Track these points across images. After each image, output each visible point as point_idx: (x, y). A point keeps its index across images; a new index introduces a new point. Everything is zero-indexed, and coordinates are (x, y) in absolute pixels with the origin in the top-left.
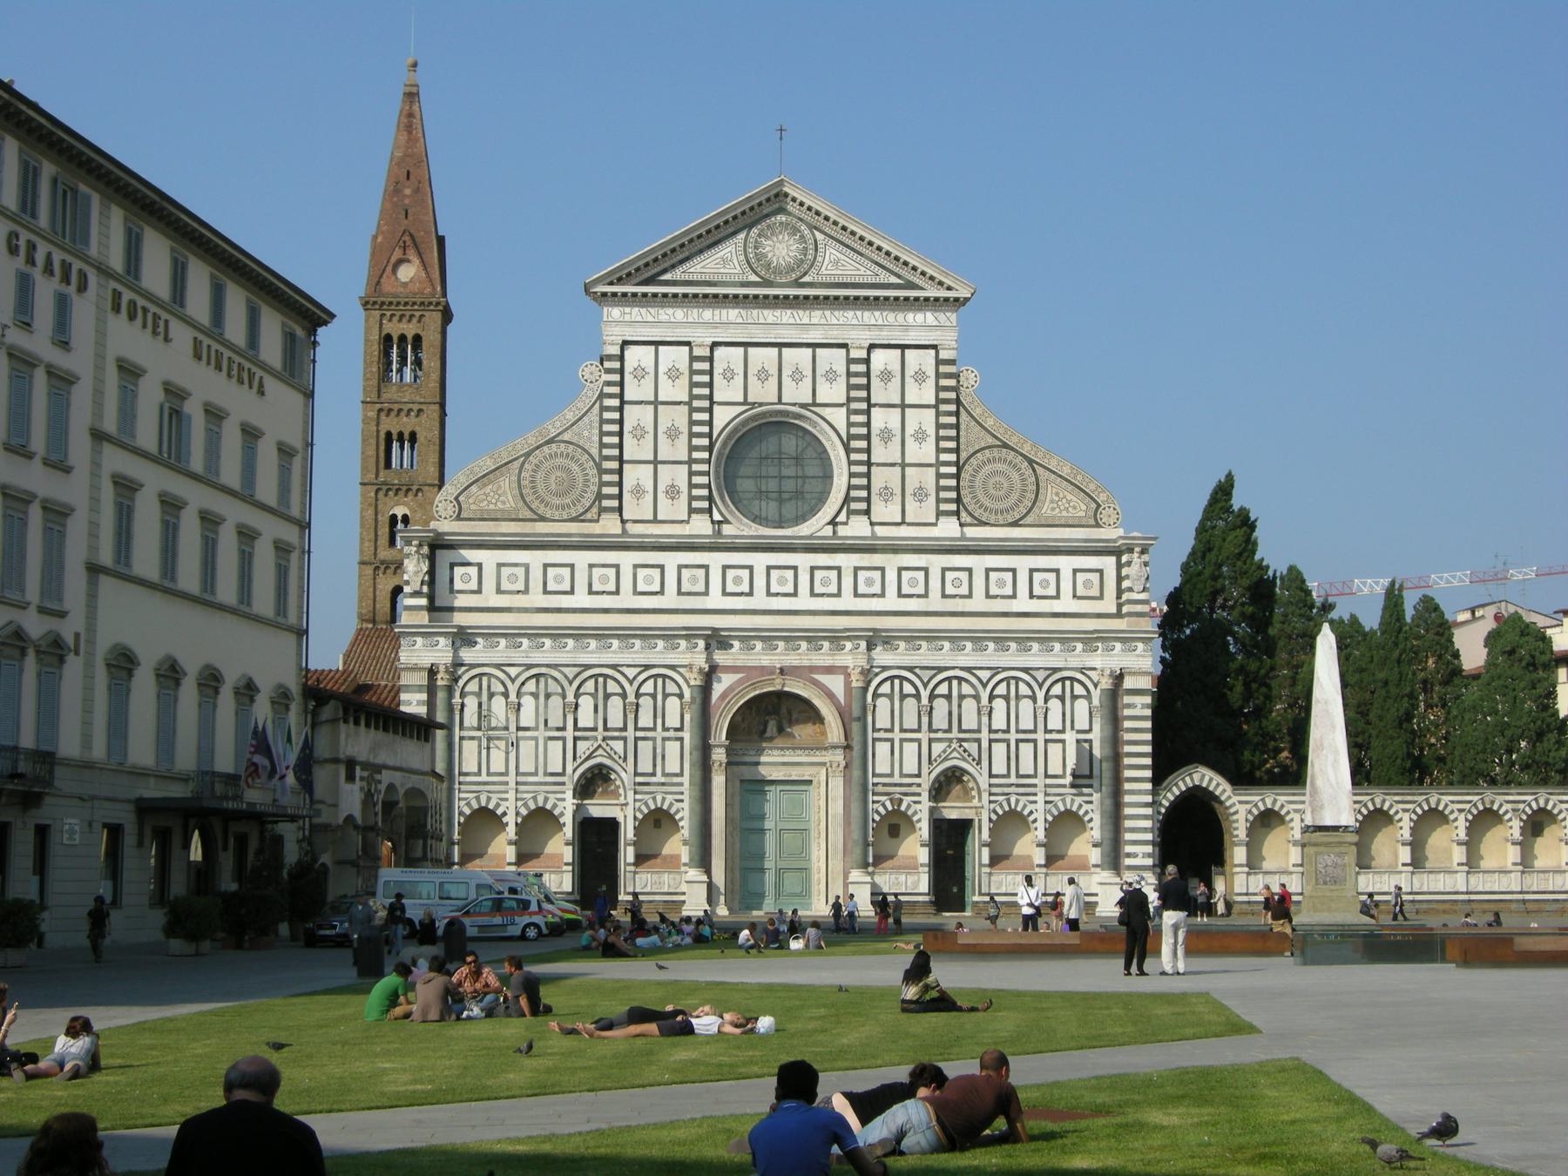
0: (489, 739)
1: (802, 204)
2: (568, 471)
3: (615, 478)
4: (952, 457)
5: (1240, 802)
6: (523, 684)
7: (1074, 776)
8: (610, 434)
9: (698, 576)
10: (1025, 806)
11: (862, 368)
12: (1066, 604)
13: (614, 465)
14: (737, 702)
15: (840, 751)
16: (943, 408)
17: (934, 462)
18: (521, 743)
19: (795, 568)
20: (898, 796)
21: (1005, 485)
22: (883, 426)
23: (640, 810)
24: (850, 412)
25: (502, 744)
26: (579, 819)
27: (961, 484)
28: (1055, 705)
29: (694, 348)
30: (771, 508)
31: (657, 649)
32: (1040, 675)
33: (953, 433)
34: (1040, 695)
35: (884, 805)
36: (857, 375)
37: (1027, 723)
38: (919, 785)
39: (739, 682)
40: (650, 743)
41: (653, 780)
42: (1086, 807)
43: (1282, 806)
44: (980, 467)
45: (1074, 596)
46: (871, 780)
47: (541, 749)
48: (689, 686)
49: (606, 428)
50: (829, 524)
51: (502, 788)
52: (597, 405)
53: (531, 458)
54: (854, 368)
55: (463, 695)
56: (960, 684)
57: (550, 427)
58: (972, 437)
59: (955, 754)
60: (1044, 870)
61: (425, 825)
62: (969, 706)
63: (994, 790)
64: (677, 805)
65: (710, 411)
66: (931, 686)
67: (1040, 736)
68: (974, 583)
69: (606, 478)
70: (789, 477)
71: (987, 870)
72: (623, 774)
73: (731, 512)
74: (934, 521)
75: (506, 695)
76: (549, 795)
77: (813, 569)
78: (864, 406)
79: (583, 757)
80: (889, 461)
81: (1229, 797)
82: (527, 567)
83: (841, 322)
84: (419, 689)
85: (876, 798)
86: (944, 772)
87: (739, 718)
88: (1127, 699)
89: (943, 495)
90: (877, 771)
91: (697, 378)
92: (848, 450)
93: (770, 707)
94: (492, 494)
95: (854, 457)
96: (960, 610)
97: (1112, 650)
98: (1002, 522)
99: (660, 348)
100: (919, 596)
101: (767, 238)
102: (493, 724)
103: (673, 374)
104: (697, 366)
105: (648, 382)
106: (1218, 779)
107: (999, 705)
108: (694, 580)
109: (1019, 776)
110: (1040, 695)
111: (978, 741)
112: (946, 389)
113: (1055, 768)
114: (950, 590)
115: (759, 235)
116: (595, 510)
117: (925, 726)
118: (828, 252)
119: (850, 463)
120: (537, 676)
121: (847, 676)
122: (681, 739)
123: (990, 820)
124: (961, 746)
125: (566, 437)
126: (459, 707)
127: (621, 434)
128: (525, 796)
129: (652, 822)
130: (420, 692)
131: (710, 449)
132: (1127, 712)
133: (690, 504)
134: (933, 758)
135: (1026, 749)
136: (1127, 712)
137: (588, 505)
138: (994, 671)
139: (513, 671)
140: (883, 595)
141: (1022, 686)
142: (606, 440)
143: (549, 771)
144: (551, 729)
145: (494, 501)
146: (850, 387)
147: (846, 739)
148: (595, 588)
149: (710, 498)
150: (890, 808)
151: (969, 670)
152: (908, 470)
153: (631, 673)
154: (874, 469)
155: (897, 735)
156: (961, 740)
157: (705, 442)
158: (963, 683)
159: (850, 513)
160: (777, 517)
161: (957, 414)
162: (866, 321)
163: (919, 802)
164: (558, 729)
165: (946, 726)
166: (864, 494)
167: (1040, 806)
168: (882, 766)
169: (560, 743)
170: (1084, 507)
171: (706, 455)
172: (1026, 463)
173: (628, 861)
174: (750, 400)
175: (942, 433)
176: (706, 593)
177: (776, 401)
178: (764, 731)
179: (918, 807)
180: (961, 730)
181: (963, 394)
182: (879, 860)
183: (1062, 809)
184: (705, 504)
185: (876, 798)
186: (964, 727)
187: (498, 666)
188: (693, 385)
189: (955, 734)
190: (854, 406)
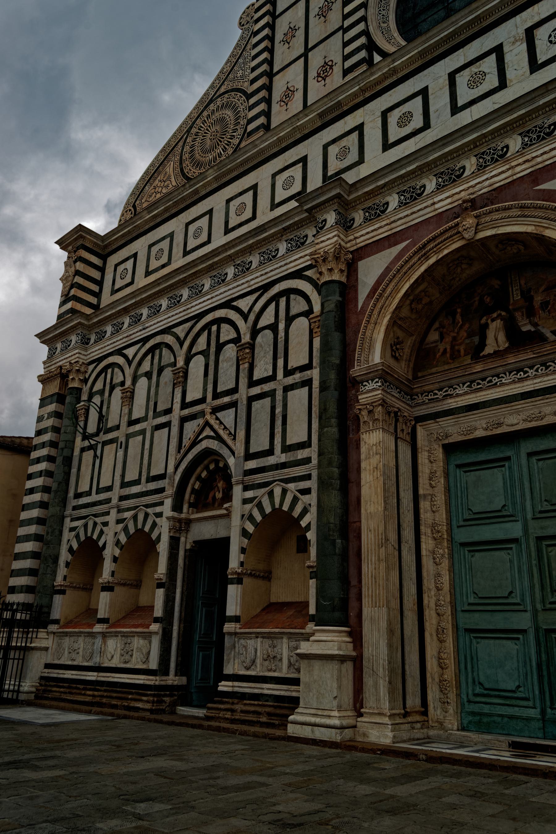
0: (105, 443)
2: (222, 120)
14: (396, 290)
23: (251, 518)
41: (271, 460)
55: (91, 396)
72: (231, 461)
75: (123, 384)
76: (150, 510)
93: (488, 300)
129: (293, 544)
130: (51, 403)
139: (130, 352)
143: (153, 473)
178: (483, 344)
187: (119, 352)
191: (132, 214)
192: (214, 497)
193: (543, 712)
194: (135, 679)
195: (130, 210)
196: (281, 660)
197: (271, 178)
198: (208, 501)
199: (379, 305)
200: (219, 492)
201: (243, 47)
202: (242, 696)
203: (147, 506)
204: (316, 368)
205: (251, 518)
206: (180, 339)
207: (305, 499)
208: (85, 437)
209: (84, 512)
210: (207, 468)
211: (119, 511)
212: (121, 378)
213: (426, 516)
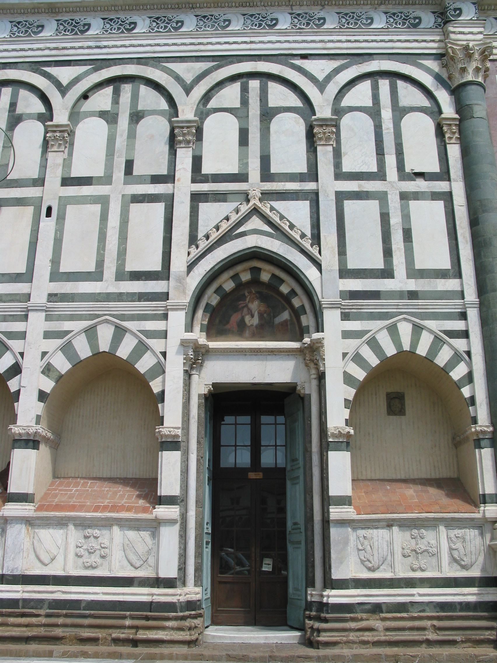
6: (85, 96)
18: (70, 210)
23: (358, 359)
25: (30, 210)
40: (373, 205)
51: (16, 307)
76: (126, 324)
79: (215, 236)
128: (67, 325)
143: (130, 267)
144: (141, 180)
164: (156, 179)
169: (160, 208)
173: (333, 491)
194: (123, 594)
198: (228, 327)
200: (253, 316)
203: (123, 317)
204: (455, 181)
205: (358, 359)
206: (183, 81)
207: (460, 344)
210: (235, 277)
211: (48, 318)
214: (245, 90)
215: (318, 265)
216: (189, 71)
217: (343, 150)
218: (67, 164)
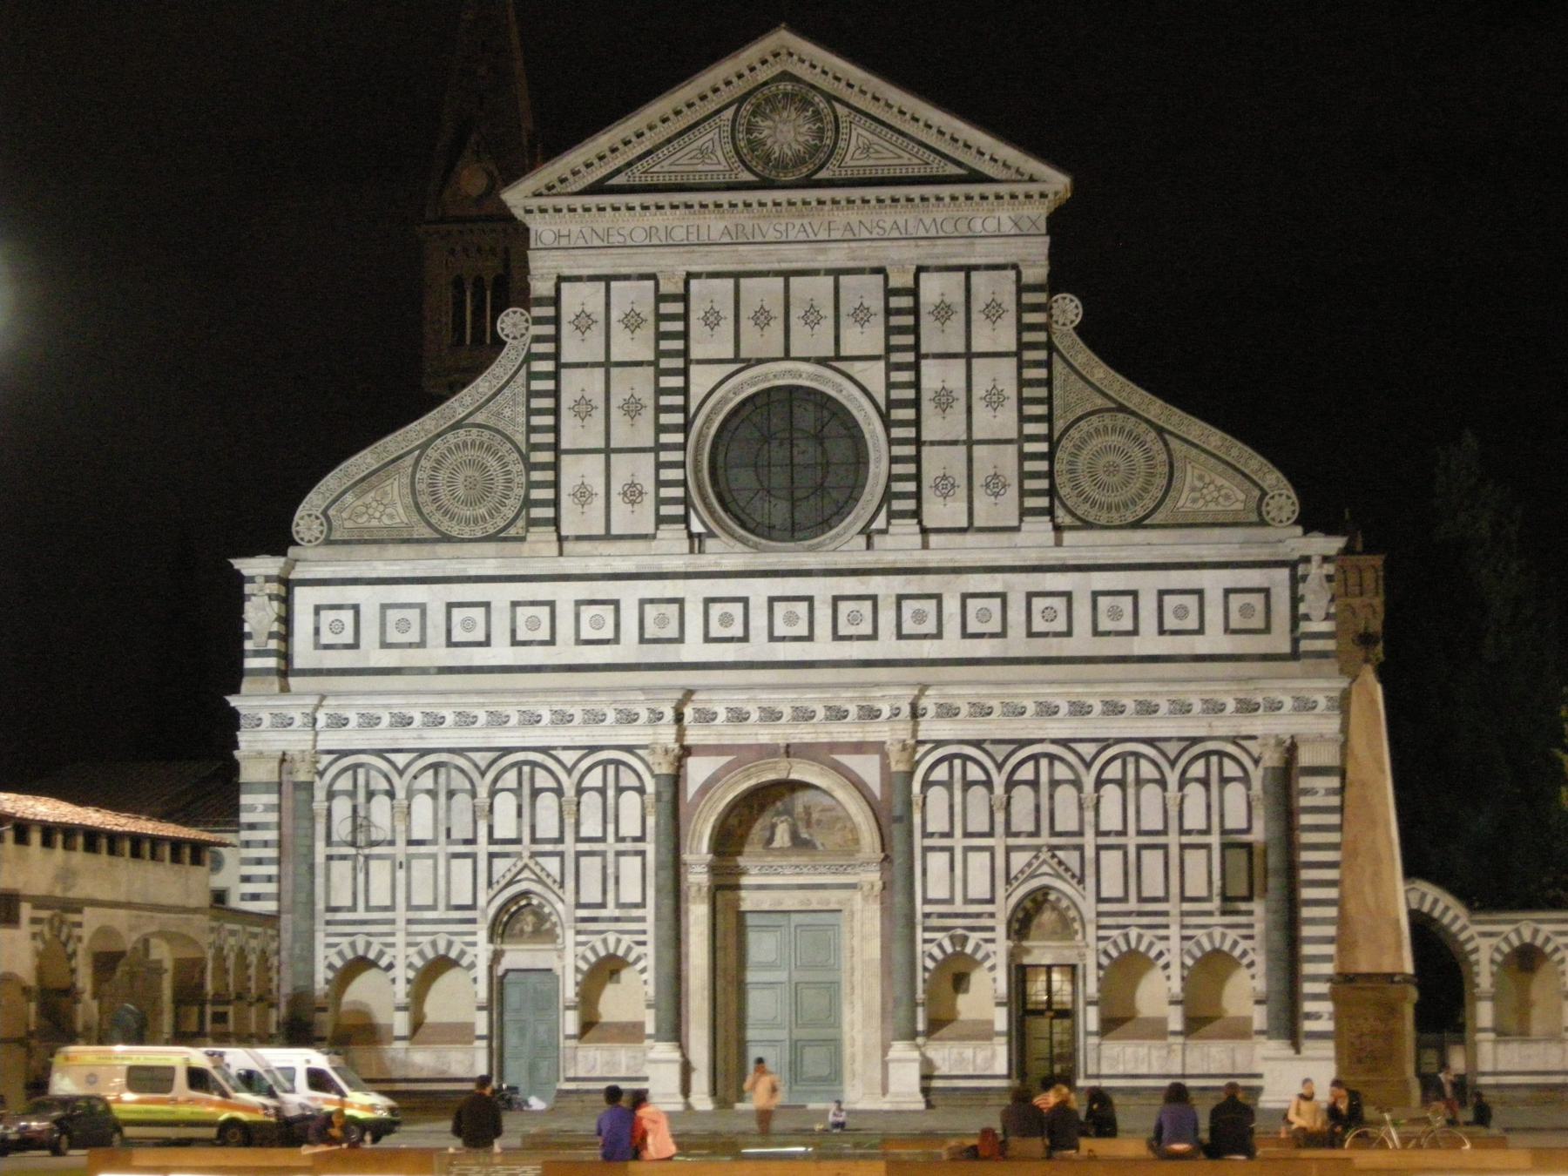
0: (367, 858)
1: (813, 66)
2: (483, 468)
3: (549, 476)
4: (1042, 428)
5: (1484, 935)
6: (415, 777)
7: (1225, 898)
8: (541, 412)
9: (668, 614)
10: (1151, 945)
11: (906, 302)
12: (1214, 641)
13: (546, 457)
15: (875, 867)
16: (1029, 355)
17: (1014, 435)
18: (414, 863)
19: (810, 600)
20: (960, 932)
21: (1122, 468)
22: (939, 386)
23: (584, 958)
24: (891, 367)
25: (388, 863)
26: (500, 971)
27: (1057, 467)
28: (1195, 792)
29: (662, 282)
30: (779, 512)
31: (607, 722)
32: (1172, 749)
33: (1042, 392)
34: (1173, 778)
35: (940, 946)
36: (900, 312)
37: (1153, 821)
38: (992, 915)
39: (727, 769)
40: (597, 860)
42: (1243, 945)
43: (1547, 940)
44: (1084, 441)
45: (1228, 630)
46: (920, 908)
47: (442, 871)
48: (654, 776)
49: (536, 403)
50: (861, 532)
52: (523, 372)
53: (429, 451)
54: (895, 302)
55: (331, 795)
56: (1051, 764)
57: (456, 405)
58: (1070, 396)
59: (1045, 869)
60: (1180, 1039)
61: (201, 986)
62: (1066, 794)
63: (1105, 921)
64: (638, 950)
65: (685, 372)
66: (1008, 767)
67: (1173, 839)
68: (1075, 614)
69: (537, 476)
70: (807, 466)
71: (1093, 1040)
72: (559, 906)
73: (718, 521)
74: (1015, 523)
75: (391, 794)
76: (454, 938)
77: (836, 600)
78: (909, 357)
79: (503, 883)
80: (948, 438)
81: (1464, 928)
82: (422, 608)
83: (874, 236)
84: (266, 787)
85: (928, 935)
86: (1030, 894)
87: (733, 821)
88: (1304, 782)
89: (1030, 484)
90: (931, 895)
91: (666, 326)
92: (888, 423)
94: (374, 504)
95: (897, 433)
96: (1054, 653)
97: (1279, 708)
98: (1117, 523)
99: (613, 284)
100: (993, 635)
101: (765, 117)
102: (374, 837)
103: (632, 322)
104: (667, 308)
105: (596, 336)
106: (1446, 899)
107: (1111, 794)
108: (662, 621)
109: (1141, 899)
110: (1173, 778)
111: (1080, 848)
112: (1033, 327)
113: (1196, 886)
114: (1039, 625)
115: (754, 114)
116: (521, 523)
117: (1000, 828)
118: (854, 134)
119: (891, 442)
120: (436, 767)
121: (885, 756)
122: (642, 853)
123: (1100, 966)
124: (1054, 856)
125: (479, 418)
126: (325, 812)
127: (556, 412)
128: (419, 939)
130: (268, 792)
131: (685, 428)
132: (1304, 801)
133: (657, 510)
134: (1012, 875)
135: (1152, 860)
136: (1304, 801)
137: (511, 515)
138: (1101, 745)
139: (401, 760)
140: (939, 635)
141: (1144, 764)
142: (536, 421)
143: (454, 902)
144: (456, 842)
145: (377, 515)
146: (890, 330)
147: (883, 850)
148: (520, 637)
149: (686, 501)
150: (949, 950)
151: (1064, 743)
152: (978, 451)
153: (569, 758)
154: (925, 450)
155: (958, 842)
156: (1053, 848)
157: (678, 418)
158: (1057, 764)
159: (892, 515)
160: (788, 524)
161: (1048, 364)
162: (912, 232)
163: (992, 941)
164: (467, 842)
165: (1031, 827)
166: (911, 487)
167: (1175, 943)
168: (938, 890)
169: (469, 861)
170: (1242, 496)
171: (678, 438)
172: (1153, 434)
174: (743, 355)
175: (1028, 392)
176: (680, 640)
177: (782, 355)
178: (771, 840)
179: (990, 947)
180: (1054, 833)
181: (1058, 334)
182: (938, 1025)
183: (1208, 947)
184: (679, 510)
185: (928, 935)
186: (1058, 828)
187: (380, 753)
188: (661, 336)
189: (1045, 839)
190: (896, 358)
191: (322, 524)
192: (522, 931)
193: (790, 1088)
195: (317, 518)
196: (620, 1065)
197: (573, 604)
199: (709, 805)
201: (510, 373)
202: (588, 1092)
205: (584, 958)
208: (329, 842)
209: (348, 929)
211: (409, 934)
212: (385, 785)
213: (720, 963)
214: (520, 773)
215: (562, 901)
216: (483, 758)
217: (583, 819)
218: (408, 829)
